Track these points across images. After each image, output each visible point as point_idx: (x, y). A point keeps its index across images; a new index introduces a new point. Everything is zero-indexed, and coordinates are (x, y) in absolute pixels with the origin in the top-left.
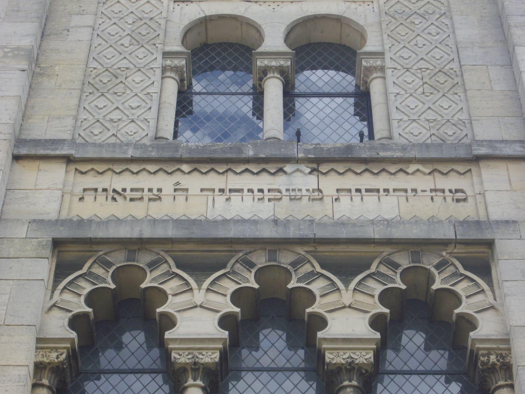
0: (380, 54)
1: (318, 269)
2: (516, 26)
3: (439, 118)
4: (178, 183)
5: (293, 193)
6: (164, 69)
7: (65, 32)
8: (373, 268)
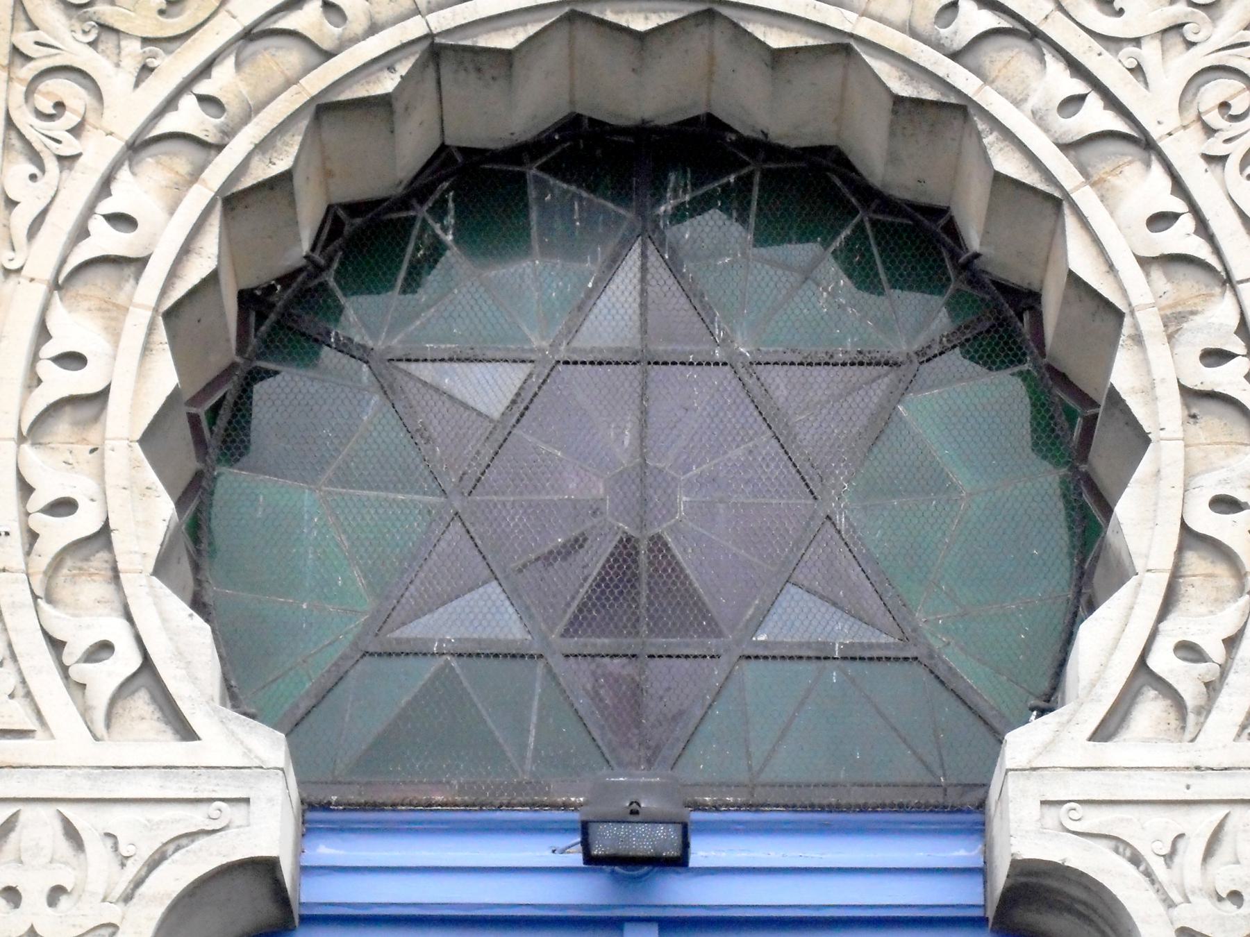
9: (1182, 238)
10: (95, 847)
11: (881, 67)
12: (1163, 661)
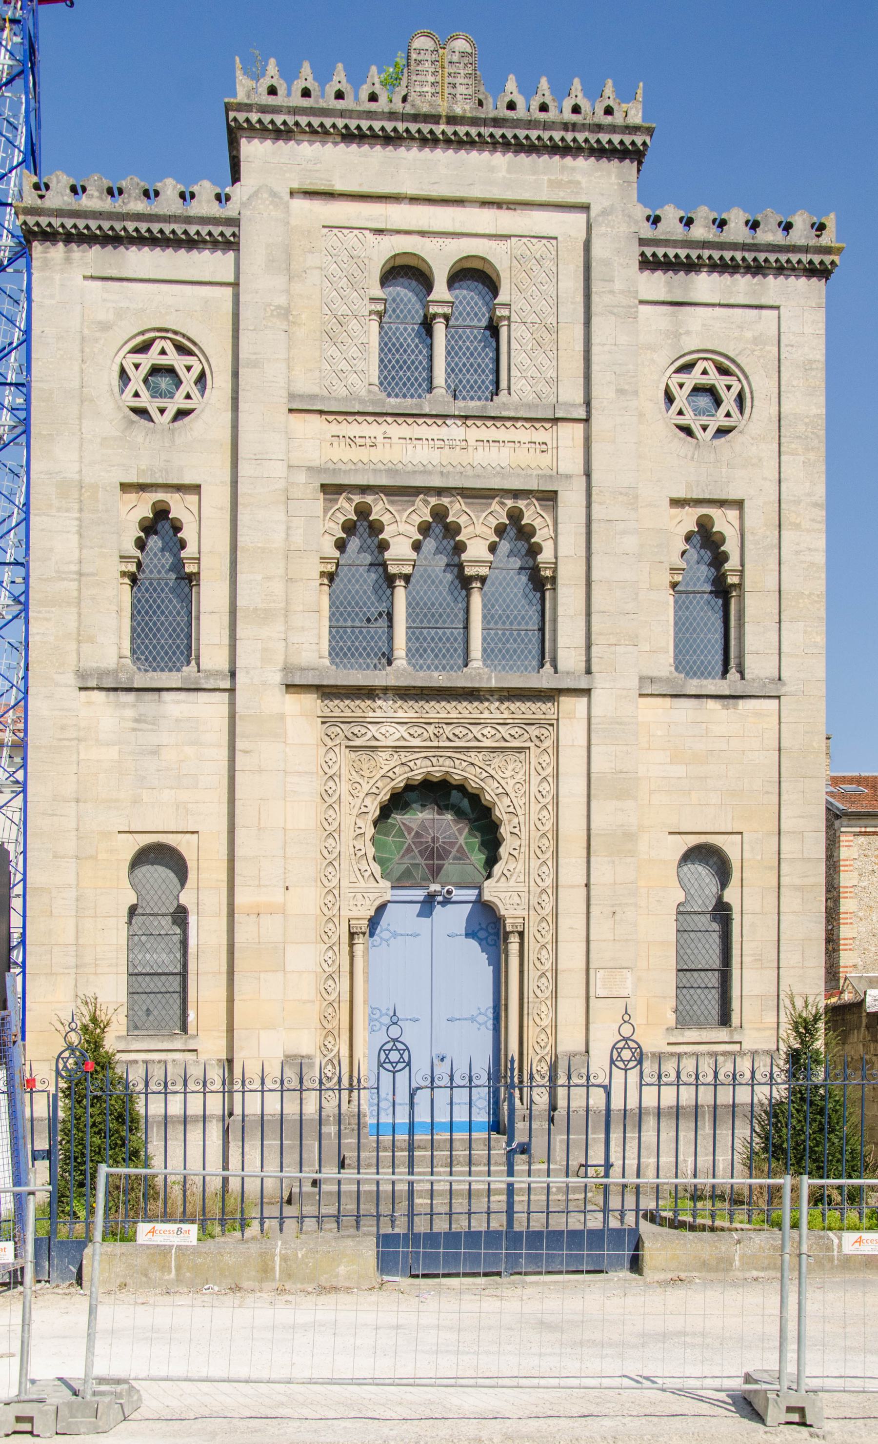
0: (508, 305)
1: (464, 508)
2: (596, 293)
3: (539, 375)
4: (385, 433)
5: (451, 443)
6: (371, 313)
7: (304, 275)
8: (492, 509)
9: (511, 809)
10: (367, 899)
11: (471, 782)
12: (505, 872)
